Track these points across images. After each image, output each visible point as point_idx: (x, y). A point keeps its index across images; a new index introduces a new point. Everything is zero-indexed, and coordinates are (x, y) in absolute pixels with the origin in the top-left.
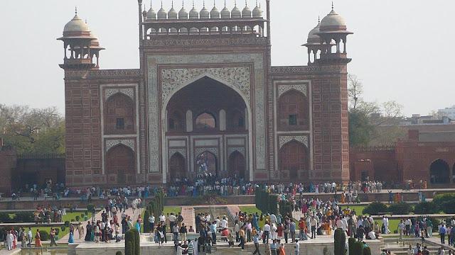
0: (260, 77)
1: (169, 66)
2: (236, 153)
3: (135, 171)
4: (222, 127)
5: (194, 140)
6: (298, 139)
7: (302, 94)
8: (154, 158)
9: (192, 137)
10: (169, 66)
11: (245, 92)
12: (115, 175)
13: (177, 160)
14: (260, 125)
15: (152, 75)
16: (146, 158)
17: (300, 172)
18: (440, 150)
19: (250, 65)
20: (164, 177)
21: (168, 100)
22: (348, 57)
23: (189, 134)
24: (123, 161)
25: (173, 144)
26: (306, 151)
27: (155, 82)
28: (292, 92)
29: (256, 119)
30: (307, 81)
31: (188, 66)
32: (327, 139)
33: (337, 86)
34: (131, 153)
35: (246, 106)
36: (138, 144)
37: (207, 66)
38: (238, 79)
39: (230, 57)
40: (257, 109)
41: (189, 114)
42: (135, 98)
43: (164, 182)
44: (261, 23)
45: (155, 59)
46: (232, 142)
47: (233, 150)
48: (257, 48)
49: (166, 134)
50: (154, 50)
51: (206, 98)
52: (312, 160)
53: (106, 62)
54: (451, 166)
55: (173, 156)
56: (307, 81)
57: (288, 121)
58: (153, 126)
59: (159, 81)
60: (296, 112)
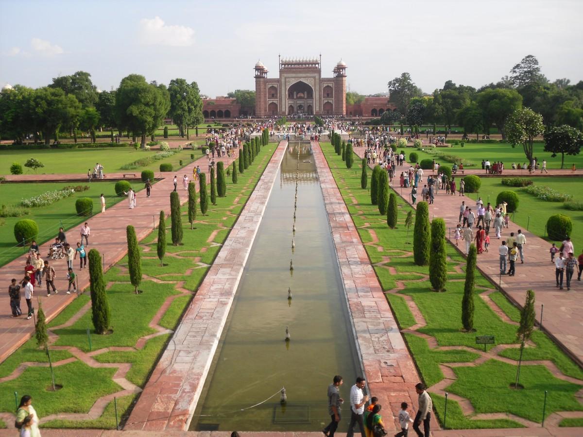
0: (317, 81)
1: (289, 78)
2: (310, 105)
4: (306, 97)
6: (329, 101)
7: (331, 87)
8: (283, 107)
10: (289, 78)
12: (271, 112)
13: (291, 107)
14: (317, 96)
15: (283, 80)
17: (330, 112)
19: (314, 78)
20: (287, 112)
23: (295, 99)
24: (274, 108)
25: (289, 102)
26: (332, 105)
28: (328, 86)
29: (316, 95)
31: (295, 78)
32: (339, 101)
33: (342, 84)
34: (276, 105)
39: (309, 75)
41: (295, 93)
43: (287, 114)
44: (318, 64)
46: (308, 102)
47: (309, 104)
51: (300, 89)
53: (269, 76)
54: (378, 110)
57: (326, 95)
58: (283, 96)
59: (285, 82)
60: (329, 92)
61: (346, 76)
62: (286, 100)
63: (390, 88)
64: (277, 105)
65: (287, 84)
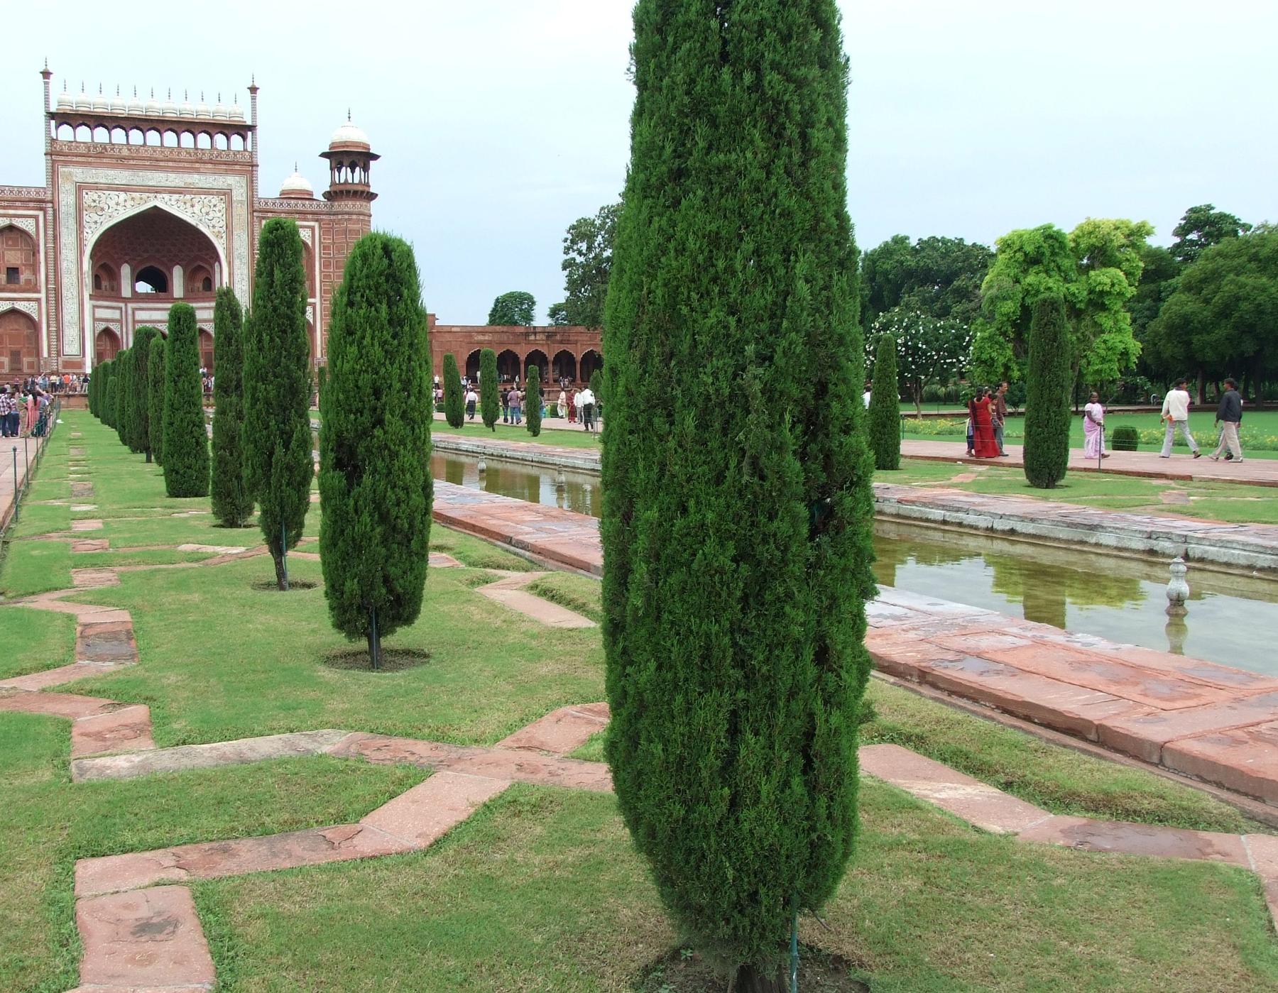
0: (241, 212)
1: (96, 187)
3: (38, 353)
5: (134, 310)
8: (71, 333)
9: (130, 306)
10: (96, 187)
11: (218, 235)
15: (67, 200)
16: (58, 331)
18: (481, 338)
19: (226, 194)
21: (96, 236)
22: (372, 190)
23: (126, 300)
25: (102, 313)
27: (72, 210)
30: (312, 224)
31: (126, 189)
35: (217, 258)
36: (44, 310)
37: (156, 190)
38: (207, 214)
40: (237, 262)
41: (126, 271)
42: (38, 234)
45: (70, 174)
48: (237, 167)
49: (91, 297)
50: (69, 158)
52: (319, 342)
55: (100, 334)
56: (312, 224)
59: (79, 209)
61: (372, 196)
62: (81, 305)
63: (573, 255)
64: (33, 324)
65: (86, 218)
